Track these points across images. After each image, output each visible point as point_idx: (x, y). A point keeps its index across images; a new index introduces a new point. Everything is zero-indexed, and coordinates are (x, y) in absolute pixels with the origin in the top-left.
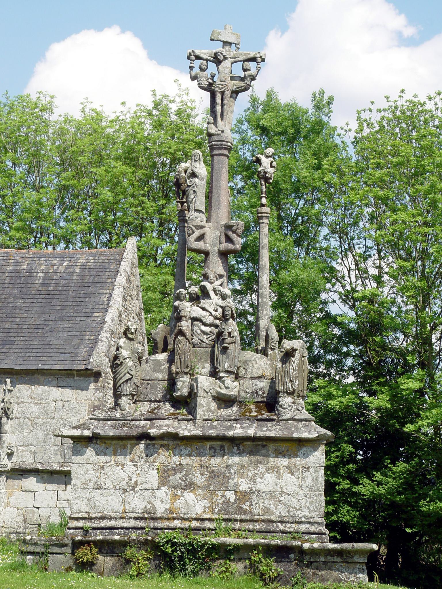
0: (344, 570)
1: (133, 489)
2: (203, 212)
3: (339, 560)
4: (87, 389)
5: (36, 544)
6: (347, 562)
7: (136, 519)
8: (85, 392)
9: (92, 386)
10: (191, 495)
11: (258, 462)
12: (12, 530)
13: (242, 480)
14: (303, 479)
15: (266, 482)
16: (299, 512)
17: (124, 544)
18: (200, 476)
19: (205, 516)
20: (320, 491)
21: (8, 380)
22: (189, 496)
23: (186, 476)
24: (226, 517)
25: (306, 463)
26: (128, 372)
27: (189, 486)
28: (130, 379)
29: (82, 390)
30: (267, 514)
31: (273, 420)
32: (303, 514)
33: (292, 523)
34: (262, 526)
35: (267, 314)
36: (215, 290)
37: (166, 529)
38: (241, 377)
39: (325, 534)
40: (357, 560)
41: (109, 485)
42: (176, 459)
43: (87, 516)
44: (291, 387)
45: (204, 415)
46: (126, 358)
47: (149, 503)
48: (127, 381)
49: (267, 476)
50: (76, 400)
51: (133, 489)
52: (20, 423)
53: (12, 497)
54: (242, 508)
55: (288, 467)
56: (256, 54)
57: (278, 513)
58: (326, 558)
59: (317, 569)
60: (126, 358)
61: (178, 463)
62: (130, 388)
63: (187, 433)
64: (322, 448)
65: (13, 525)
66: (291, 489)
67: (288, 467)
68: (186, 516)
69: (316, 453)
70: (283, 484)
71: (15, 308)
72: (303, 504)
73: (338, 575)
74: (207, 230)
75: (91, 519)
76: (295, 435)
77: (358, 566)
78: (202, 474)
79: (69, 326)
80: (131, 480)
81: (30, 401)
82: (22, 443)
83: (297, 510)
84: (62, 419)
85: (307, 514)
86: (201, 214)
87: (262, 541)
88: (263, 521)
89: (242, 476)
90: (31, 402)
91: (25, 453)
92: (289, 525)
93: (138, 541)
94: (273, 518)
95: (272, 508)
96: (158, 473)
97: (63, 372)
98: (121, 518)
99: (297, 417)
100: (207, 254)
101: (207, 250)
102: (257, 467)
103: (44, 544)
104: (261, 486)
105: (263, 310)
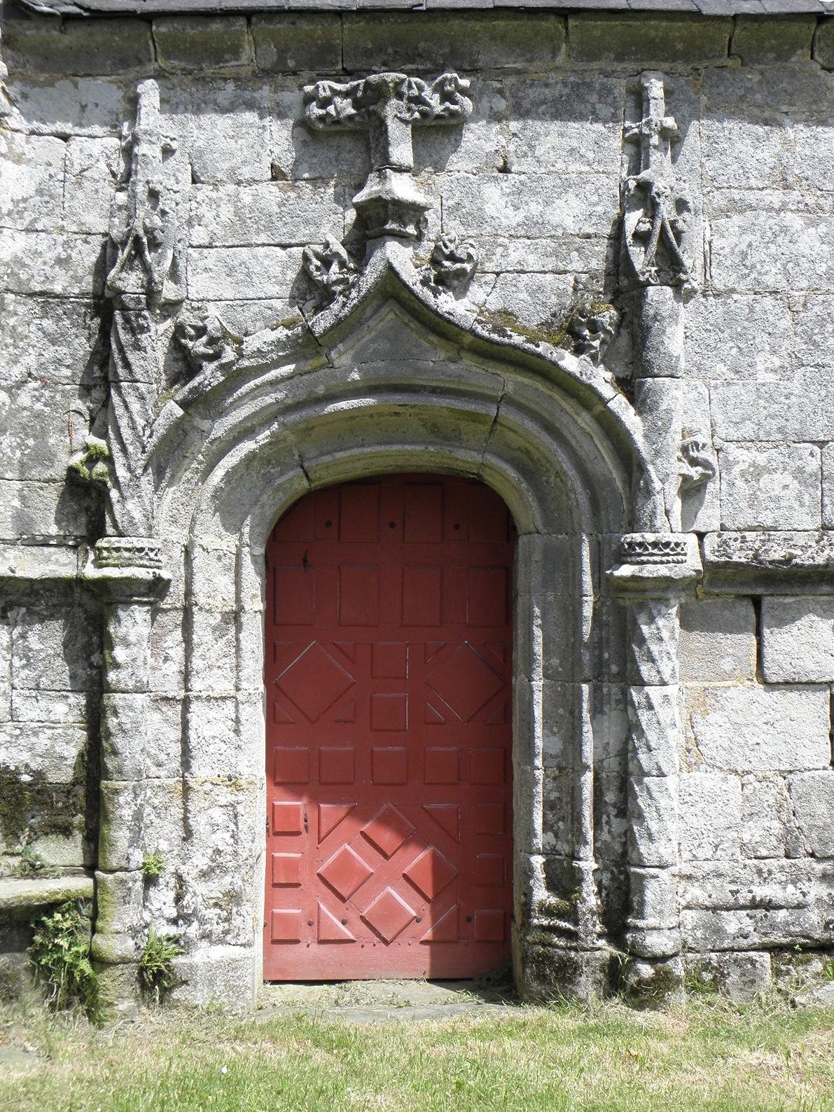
12: (720, 892)
21: (656, 88)
52: (730, 318)
53: (713, 717)
65: (724, 866)
81: (775, 197)
82: (748, 430)
90: (783, 208)
91: (775, 483)
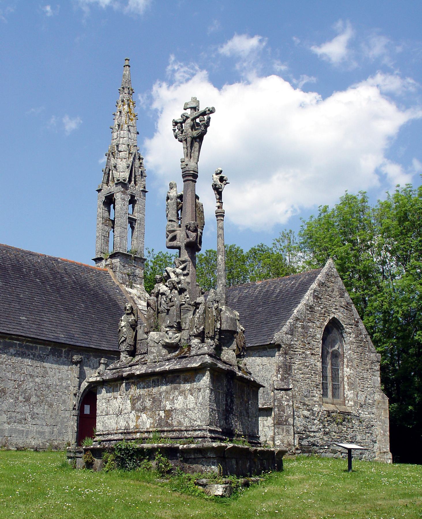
0: (204, 464)
1: (120, 414)
2: (174, 221)
3: (201, 456)
4: (274, 356)
5: (70, 452)
6: (205, 457)
7: (121, 433)
8: (273, 358)
9: (277, 354)
10: (145, 415)
11: (176, 389)
13: (167, 402)
14: (198, 398)
15: (179, 403)
16: (196, 422)
17: (103, 450)
18: (148, 402)
19: (151, 430)
20: (206, 406)
22: (144, 416)
23: (142, 402)
24: (159, 429)
25: (199, 386)
26: (123, 336)
27: (144, 409)
28: (125, 340)
29: (272, 357)
30: (180, 426)
31: (187, 357)
32: (198, 423)
33: (192, 431)
34: (175, 434)
35: (221, 283)
36: (174, 272)
37: (132, 440)
38: (183, 329)
39: (207, 438)
40: (209, 456)
41: (111, 412)
42: (138, 391)
43: (102, 433)
44: (196, 331)
45: (155, 358)
46: (122, 327)
47: (127, 422)
48: (123, 342)
49: (180, 397)
50: (269, 364)
51: (120, 414)
54: (167, 422)
55: (190, 390)
56: (206, 109)
57: (185, 424)
58: (194, 456)
59: (191, 464)
60: (122, 327)
61: (139, 394)
62: (125, 346)
63: (138, 373)
64: (208, 373)
66: (192, 406)
67: (190, 390)
68: (142, 430)
69: (204, 378)
70: (188, 403)
71: (259, 313)
72: (197, 417)
73: (201, 467)
74: (178, 233)
75: (104, 435)
76: (189, 366)
77: (212, 460)
78: (149, 400)
79: (276, 319)
80: (120, 408)
83: (195, 421)
84: (262, 376)
85: (199, 423)
86: (173, 223)
87: (160, 445)
88: (178, 431)
89: (167, 399)
92: (190, 433)
93: (109, 448)
94: (183, 428)
95: (182, 420)
96: (130, 402)
97: (260, 347)
98: (116, 433)
99: (199, 353)
100: (179, 248)
101: (178, 245)
102: (174, 392)
103: (73, 452)
104: (177, 406)
105: (219, 281)
